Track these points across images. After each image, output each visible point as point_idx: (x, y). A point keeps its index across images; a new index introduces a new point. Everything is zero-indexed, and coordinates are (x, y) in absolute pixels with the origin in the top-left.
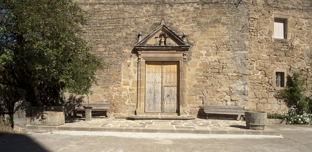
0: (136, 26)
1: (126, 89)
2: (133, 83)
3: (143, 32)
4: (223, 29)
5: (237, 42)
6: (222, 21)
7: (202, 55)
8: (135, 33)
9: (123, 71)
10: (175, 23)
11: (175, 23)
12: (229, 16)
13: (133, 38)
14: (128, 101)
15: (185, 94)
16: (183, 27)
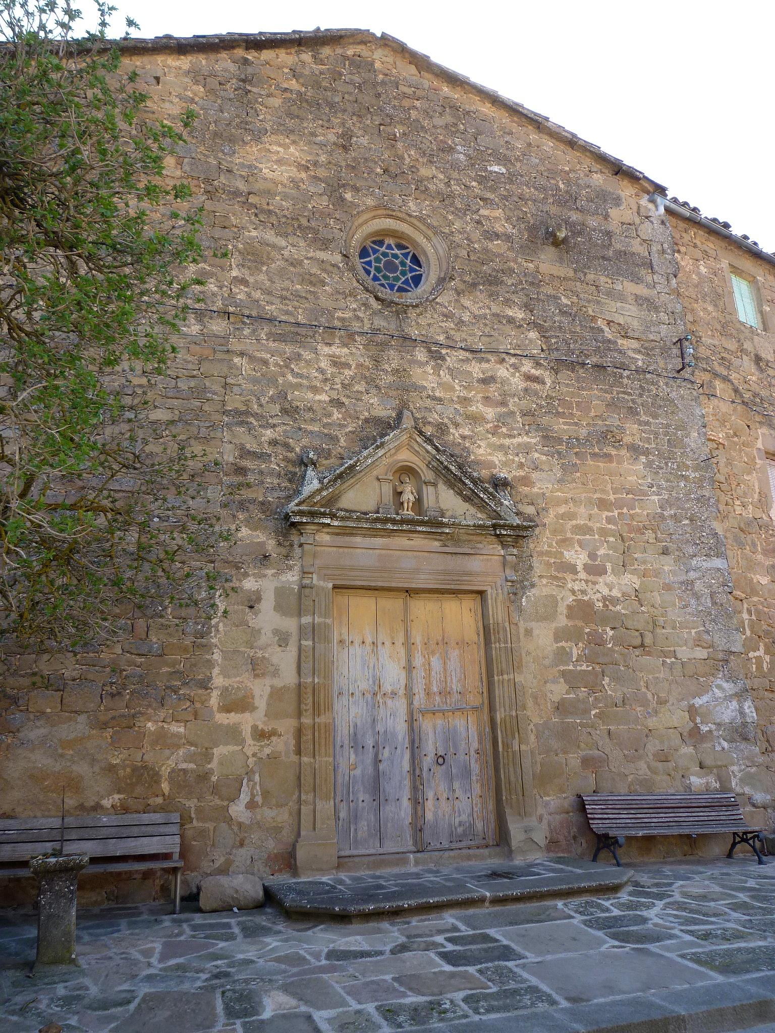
0: (287, 419)
1: (233, 734)
2: (271, 695)
3: (319, 451)
4: (634, 472)
5: (687, 522)
6: (627, 439)
7: (573, 569)
8: (279, 449)
9: (221, 633)
10: (457, 425)
11: (457, 425)
12: (647, 423)
13: (271, 473)
14: (244, 798)
15: (523, 747)
16: (489, 445)
